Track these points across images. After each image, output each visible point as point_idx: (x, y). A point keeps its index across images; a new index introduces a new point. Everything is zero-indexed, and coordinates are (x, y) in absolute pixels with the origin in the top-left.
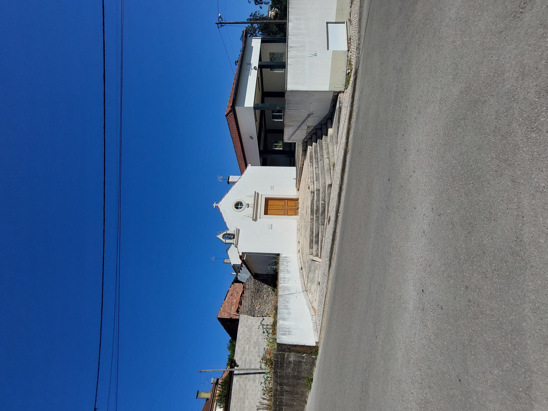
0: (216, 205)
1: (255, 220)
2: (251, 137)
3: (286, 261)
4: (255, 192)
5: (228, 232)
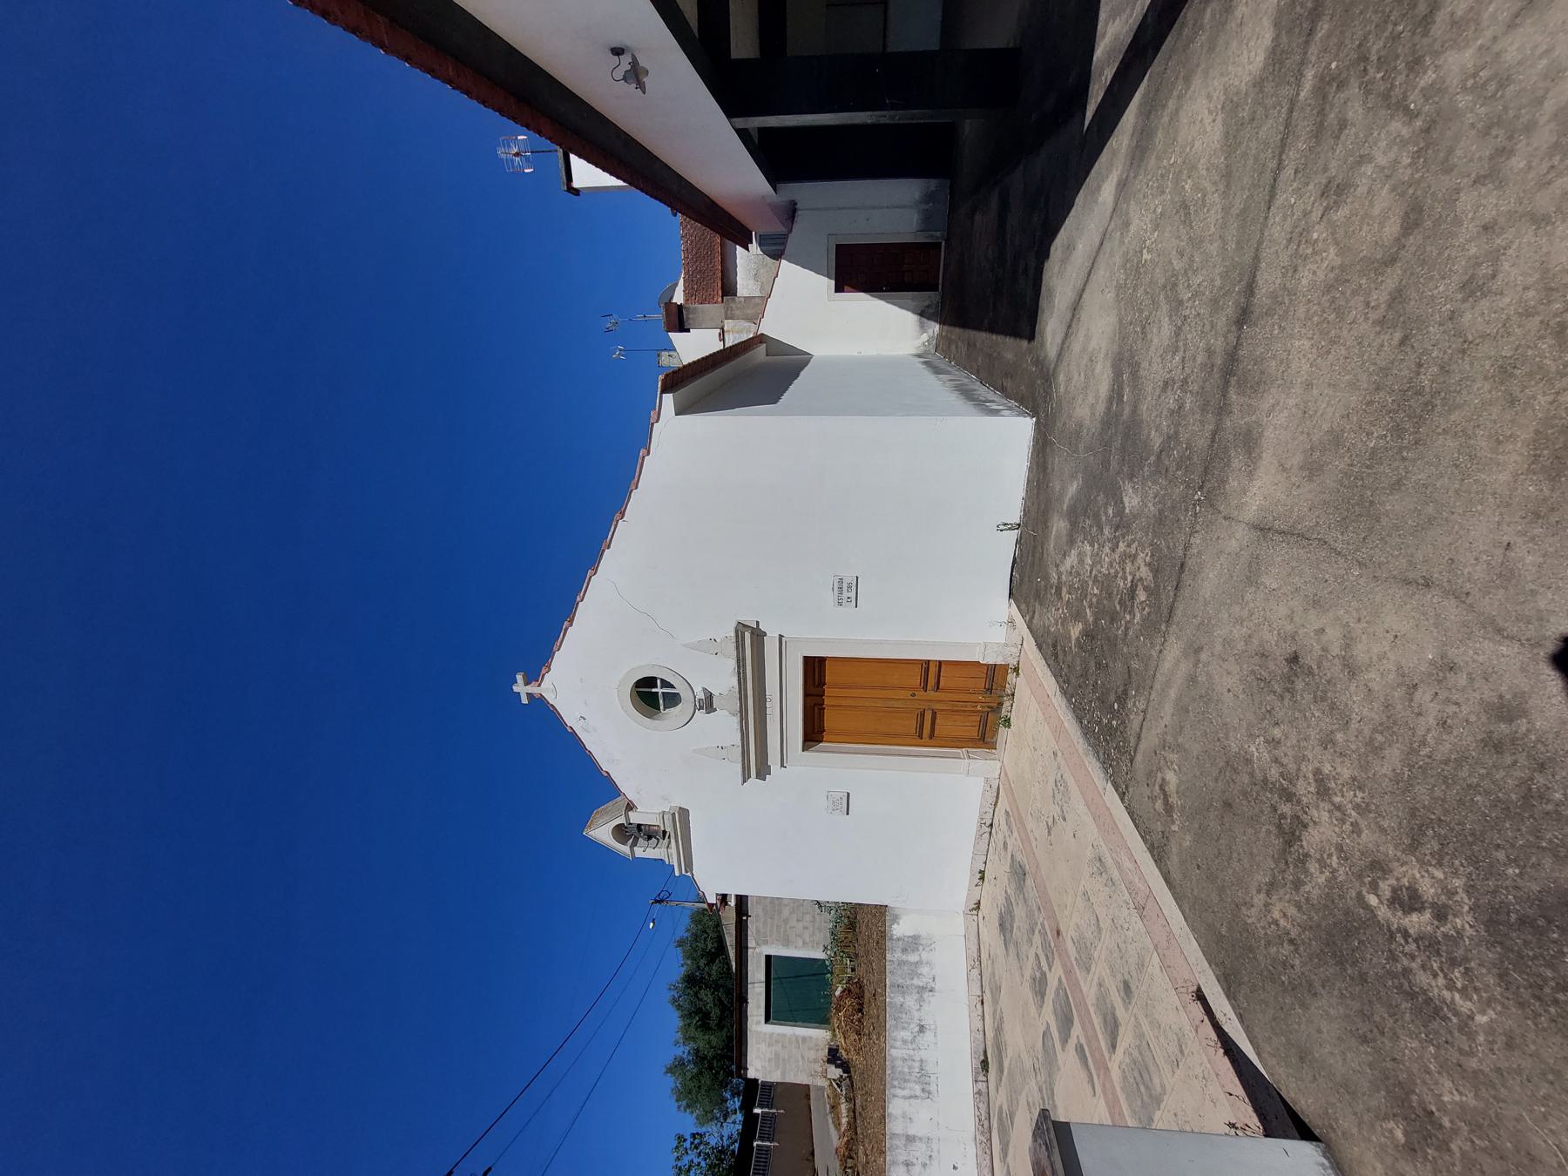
0: (532, 689)
1: (763, 772)
2: (618, 52)
3: (916, 982)
4: (741, 628)
5: (635, 818)
